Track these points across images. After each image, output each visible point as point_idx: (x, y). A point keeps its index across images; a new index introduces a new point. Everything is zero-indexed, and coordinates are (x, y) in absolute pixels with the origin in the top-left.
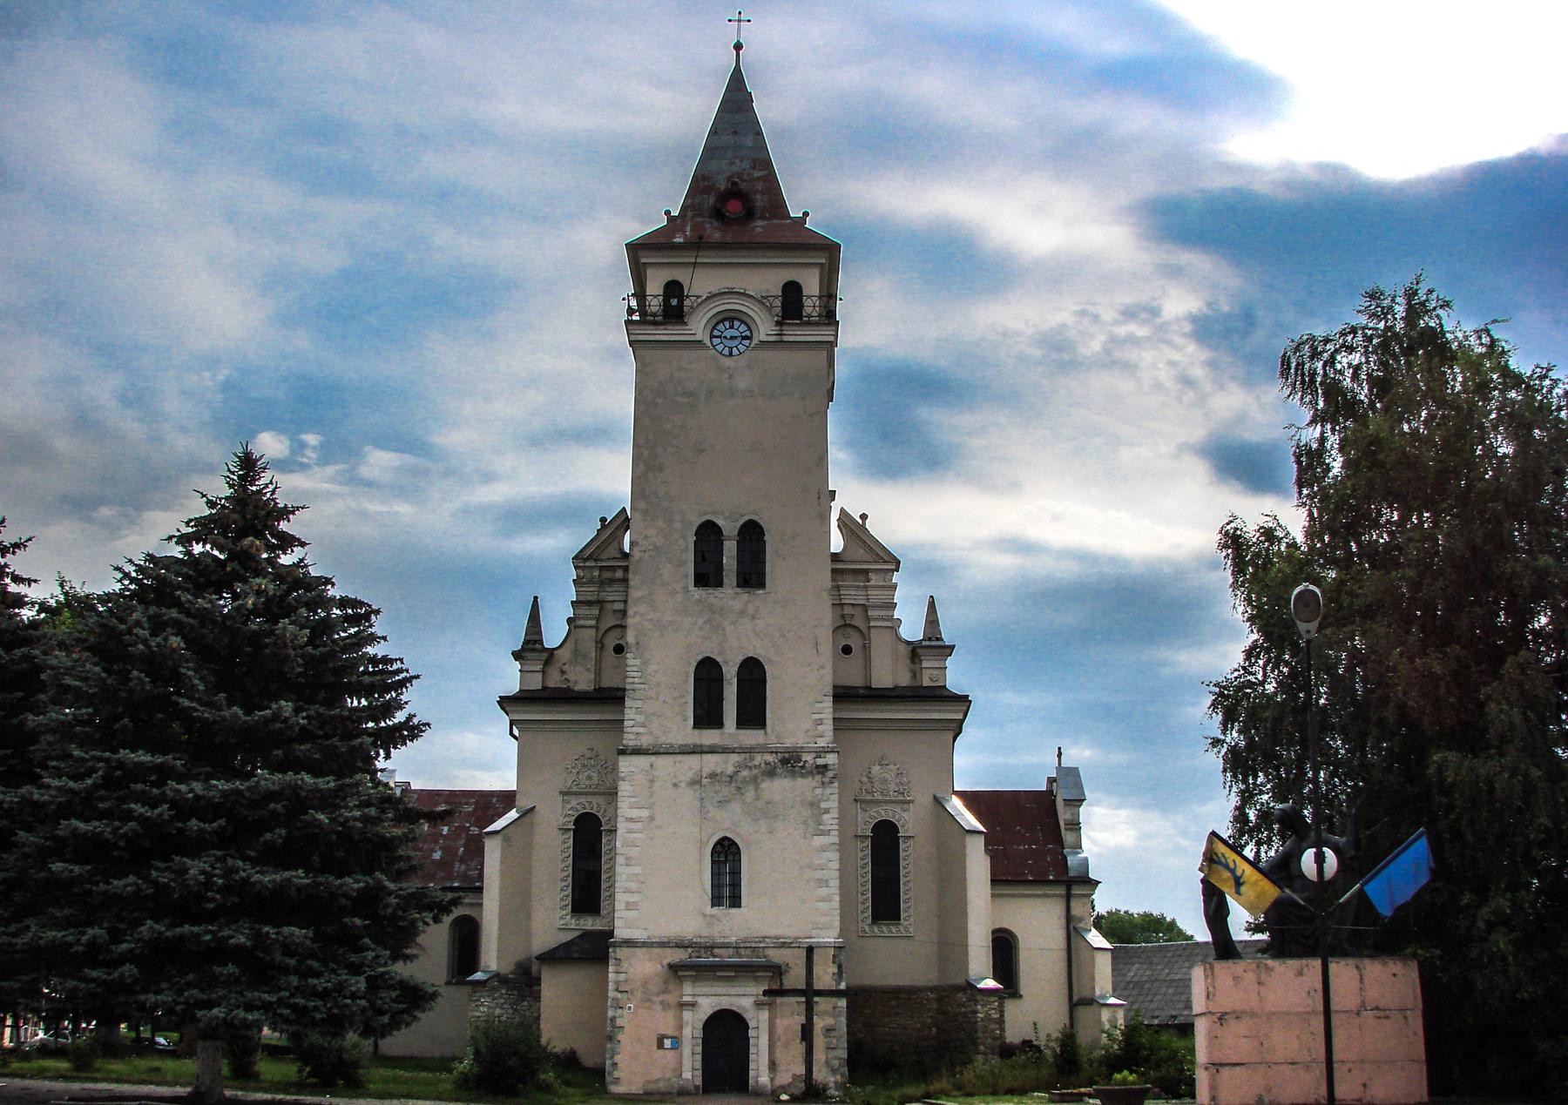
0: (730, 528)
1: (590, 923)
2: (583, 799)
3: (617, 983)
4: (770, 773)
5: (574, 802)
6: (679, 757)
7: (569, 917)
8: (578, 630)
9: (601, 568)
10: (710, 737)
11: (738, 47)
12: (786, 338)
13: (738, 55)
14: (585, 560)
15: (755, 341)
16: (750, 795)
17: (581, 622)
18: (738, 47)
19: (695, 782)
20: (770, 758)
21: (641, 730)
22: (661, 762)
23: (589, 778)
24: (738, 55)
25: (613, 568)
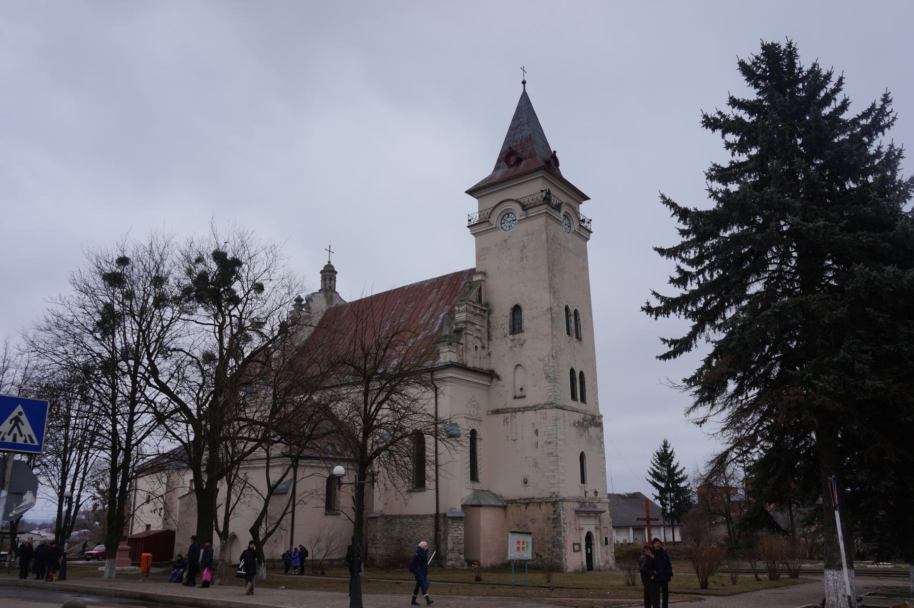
0: (572, 312)
1: (477, 486)
2: (472, 422)
3: (564, 519)
4: (590, 424)
5: (470, 422)
6: (570, 412)
7: (469, 483)
8: (468, 335)
9: (474, 307)
10: (574, 404)
11: (524, 83)
12: (581, 233)
13: (524, 86)
14: (470, 301)
15: (572, 230)
16: (587, 432)
17: (468, 332)
18: (524, 83)
19: (574, 425)
20: (589, 417)
21: (559, 398)
22: (566, 413)
23: (473, 411)
24: (524, 86)
25: (475, 308)
